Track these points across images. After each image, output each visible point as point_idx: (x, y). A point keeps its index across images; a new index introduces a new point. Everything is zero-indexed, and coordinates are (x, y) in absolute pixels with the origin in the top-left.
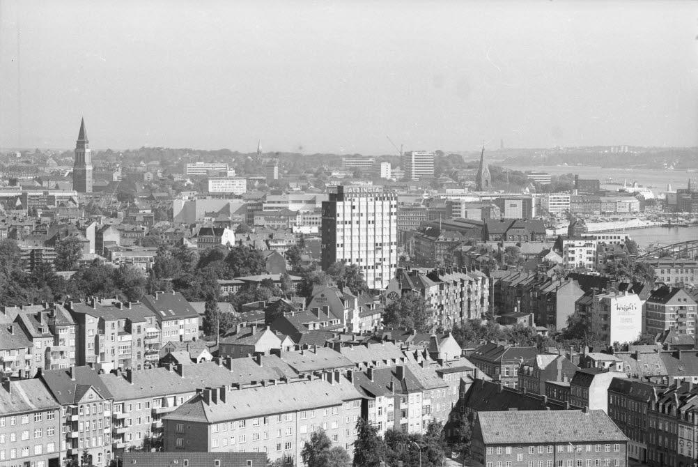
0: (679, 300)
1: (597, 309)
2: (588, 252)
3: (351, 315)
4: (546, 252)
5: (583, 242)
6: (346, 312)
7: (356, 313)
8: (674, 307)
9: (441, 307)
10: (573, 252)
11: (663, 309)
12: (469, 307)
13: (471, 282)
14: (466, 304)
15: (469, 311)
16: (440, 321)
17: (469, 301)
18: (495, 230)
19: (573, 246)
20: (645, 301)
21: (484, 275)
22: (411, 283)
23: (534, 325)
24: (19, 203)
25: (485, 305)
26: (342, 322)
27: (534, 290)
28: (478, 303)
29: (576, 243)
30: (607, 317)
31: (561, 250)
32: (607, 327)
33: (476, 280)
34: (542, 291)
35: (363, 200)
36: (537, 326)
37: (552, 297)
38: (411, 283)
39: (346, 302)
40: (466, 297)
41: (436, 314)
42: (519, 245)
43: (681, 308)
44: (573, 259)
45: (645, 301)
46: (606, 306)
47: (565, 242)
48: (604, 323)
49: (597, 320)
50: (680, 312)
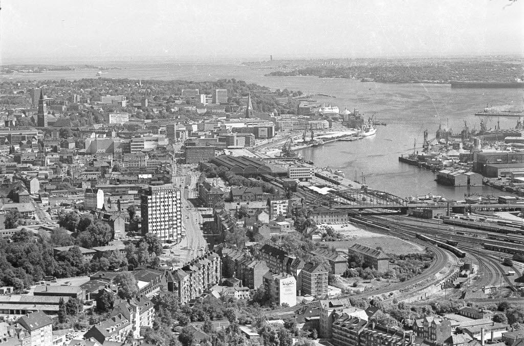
0: (319, 270)
1: (273, 284)
2: (284, 206)
3: (134, 317)
4: (259, 211)
5: (281, 202)
6: (131, 316)
7: (137, 315)
8: (316, 275)
9: (191, 285)
10: (276, 207)
11: (310, 276)
12: (208, 277)
13: (209, 264)
14: (206, 277)
15: (208, 279)
16: (191, 293)
17: (208, 274)
18: (236, 194)
19: (276, 203)
20: (301, 270)
21: (217, 255)
22: (173, 278)
23: (242, 286)
24: (7, 140)
25: (218, 271)
26: (129, 321)
27: (243, 265)
28: (214, 273)
29: (278, 202)
30: (278, 289)
31: (270, 206)
32: (278, 294)
33: (212, 261)
34: (247, 266)
35: (162, 193)
36: (244, 286)
37: (252, 270)
38: (173, 278)
39: (132, 310)
40: (206, 273)
41: (188, 290)
42: (248, 204)
43: (320, 274)
44: (276, 210)
45: (301, 270)
46: (277, 282)
47: (272, 202)
48: (277, 292)
49: (273, 291)
50: (319, 277)
